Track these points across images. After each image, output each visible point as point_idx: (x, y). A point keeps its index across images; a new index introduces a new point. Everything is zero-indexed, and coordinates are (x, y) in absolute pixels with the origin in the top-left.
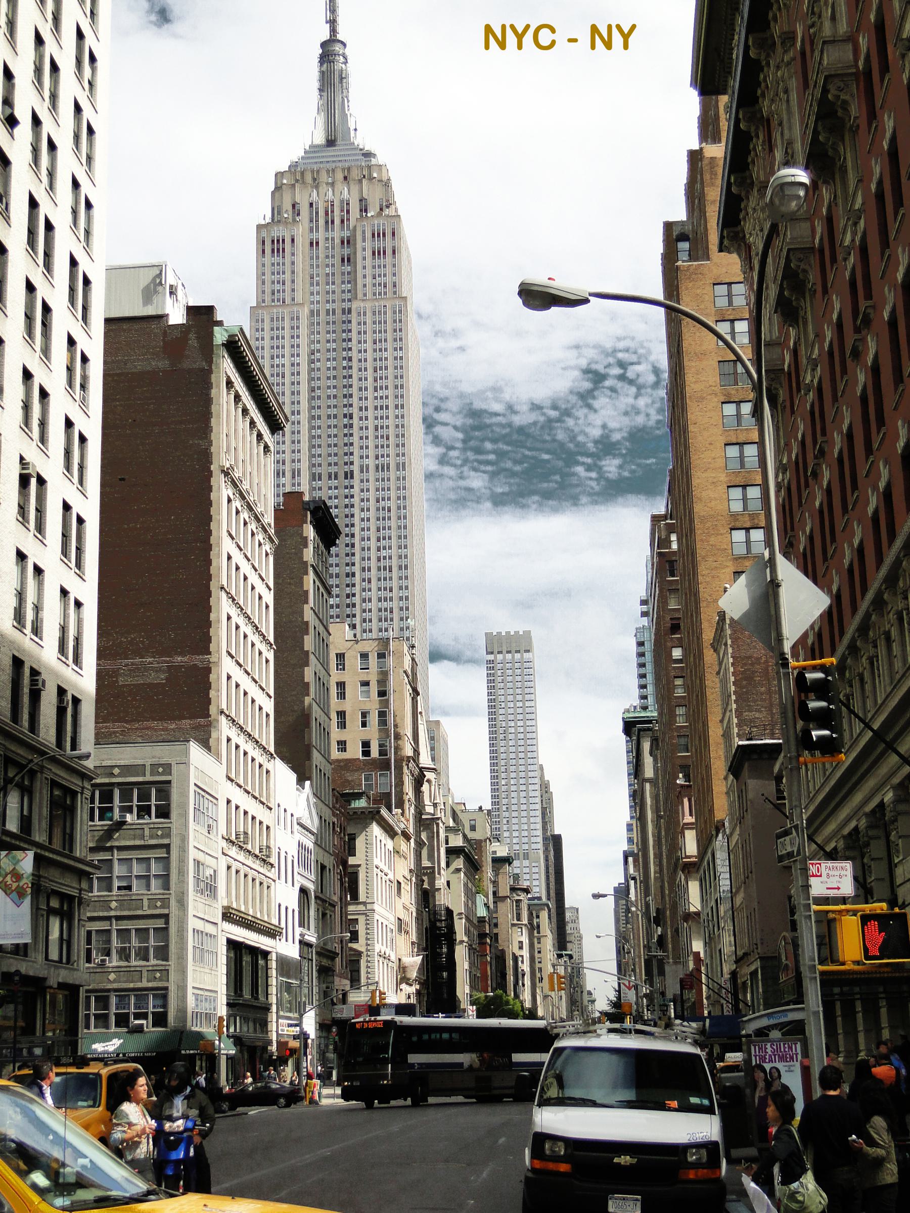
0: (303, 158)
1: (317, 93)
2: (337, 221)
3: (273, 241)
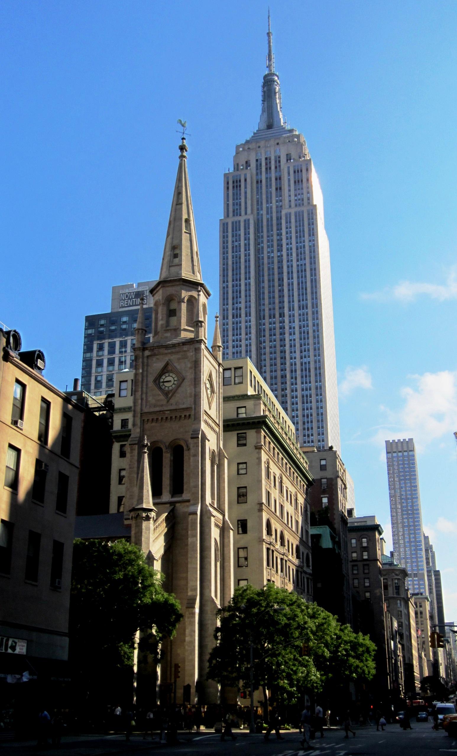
0: (252, 137)
1: (261, 102)
2: (273, 167)
3: (233, 182)
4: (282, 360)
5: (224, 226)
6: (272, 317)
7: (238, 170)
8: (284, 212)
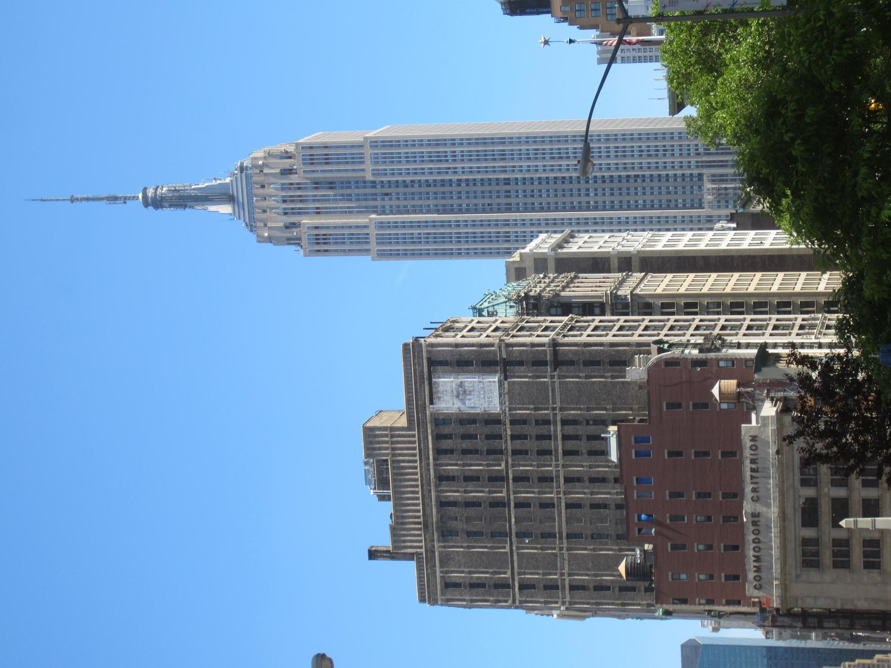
1: (187, 209)
3: (317, 243)
4: (566, 182)
5: (383, 255)
6: (508, 194)
7: (300, 239)
8: (369, 177)
